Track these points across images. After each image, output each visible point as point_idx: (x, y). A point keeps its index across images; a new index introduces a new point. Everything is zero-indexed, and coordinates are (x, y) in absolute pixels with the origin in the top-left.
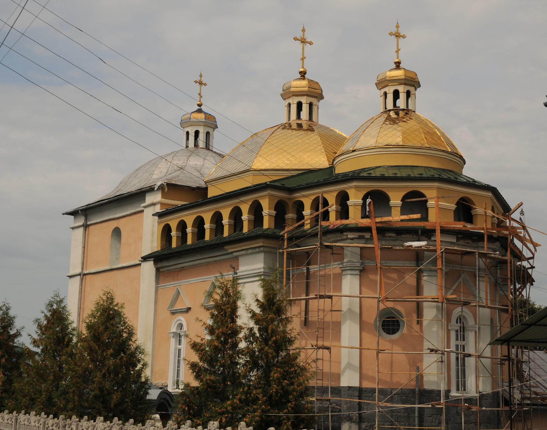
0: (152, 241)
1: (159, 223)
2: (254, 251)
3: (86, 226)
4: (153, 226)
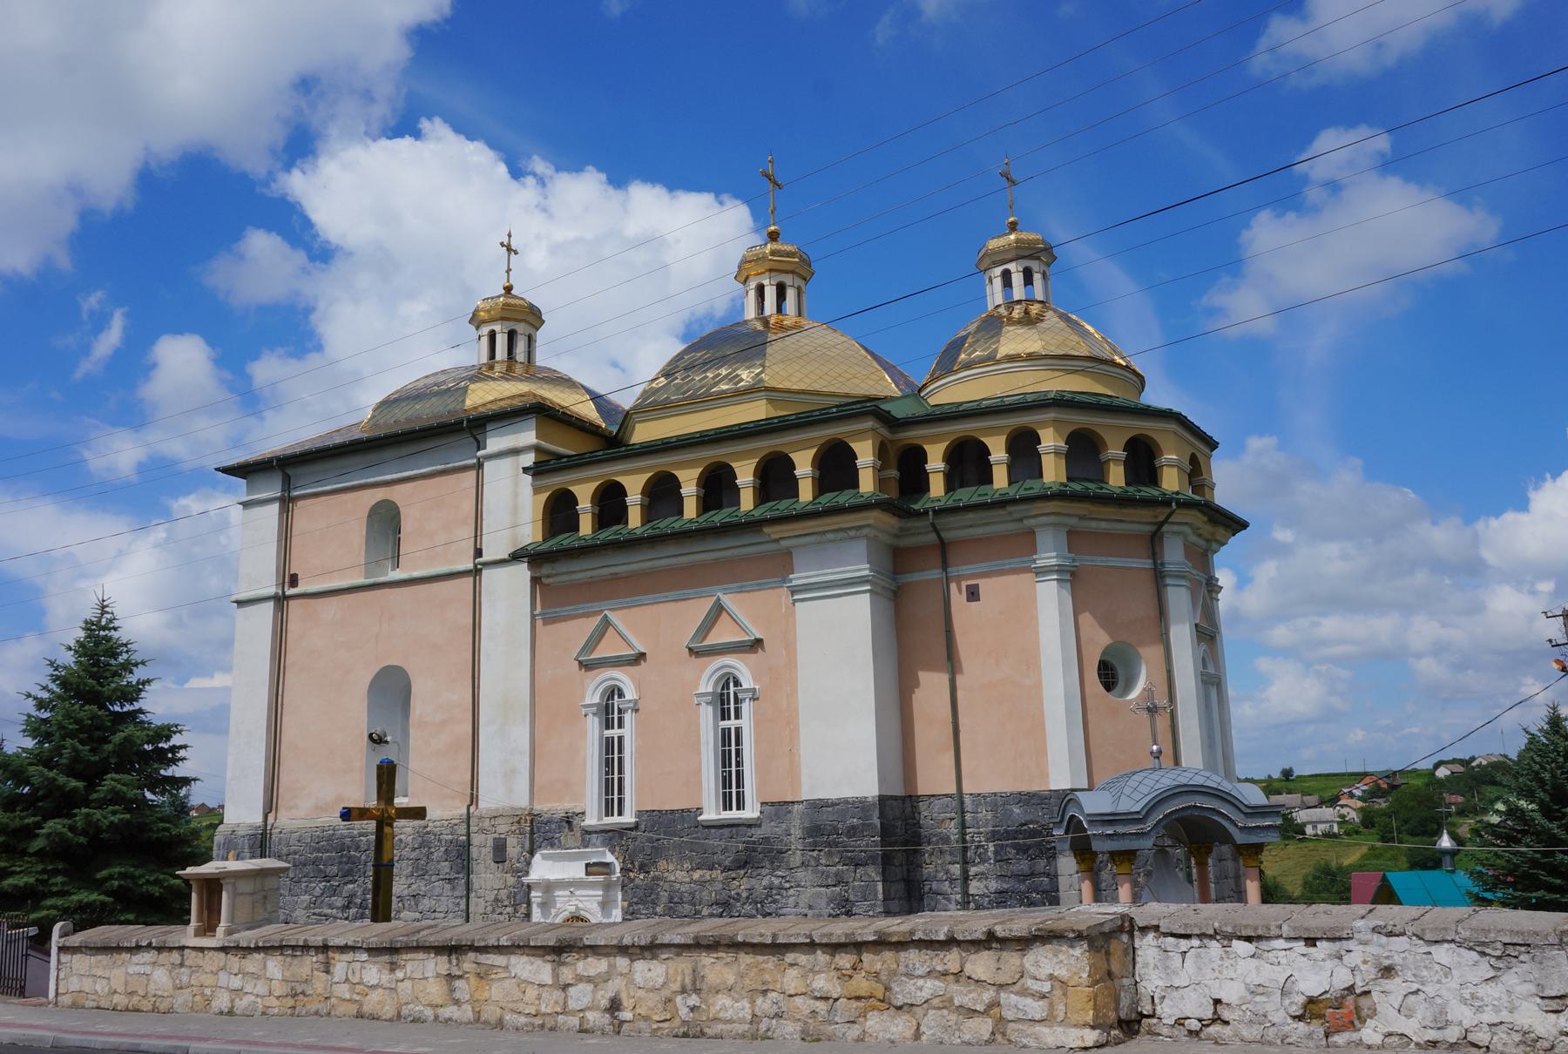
1: (537, 491)
3: (286, 502)
4: (516, 495)
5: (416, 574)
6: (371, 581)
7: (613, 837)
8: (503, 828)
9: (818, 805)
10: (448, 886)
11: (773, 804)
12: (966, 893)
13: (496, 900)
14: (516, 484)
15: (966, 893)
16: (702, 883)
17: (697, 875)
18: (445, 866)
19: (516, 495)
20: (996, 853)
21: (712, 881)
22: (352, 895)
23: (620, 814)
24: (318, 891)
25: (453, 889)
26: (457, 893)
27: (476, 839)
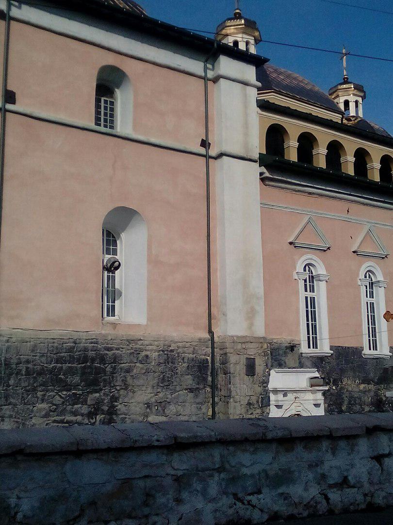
0: (246, 135)
4: (246, 115)
7: (319, 362)
8: (252, 351)
10: (191, 395)
13: (249, 404)
16: (364, 392)
17: (362, 386)
18: (189, 380)
19: (246, 115)
21: (370, 390)
22: (98, 404)
24: (58, 400)
25: (196, 396)
27: (233, 359)
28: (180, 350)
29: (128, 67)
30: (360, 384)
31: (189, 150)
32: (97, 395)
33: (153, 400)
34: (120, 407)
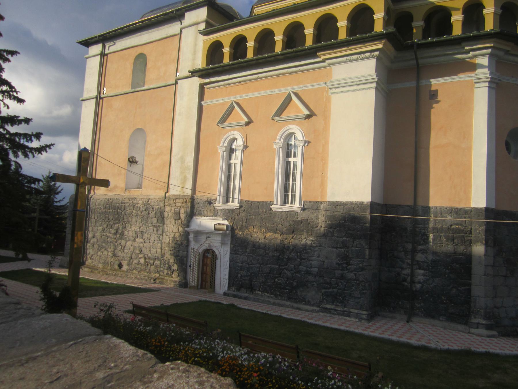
0: (194, 59)
1: (205, 42)
2: (363, 56)
4: (196, 45)
5: (152, 86)
6: (133, 90)
9: (335, 205)
10: (155, 229)
11: (310, 202)
12: (413, 259)
14: (196, 39)
15: (413, 259)
18: (155, 220)
19: (196, 45)
20: (434, 239)
23: (233, 202)
25: (157, 230)
26: (159, 233)
28: (152, 204)
29: (145, 50)
30: (266, 232)
31: (168, 84)
32: (118, 225)
33: (138, 230)
34: (126, 233)
